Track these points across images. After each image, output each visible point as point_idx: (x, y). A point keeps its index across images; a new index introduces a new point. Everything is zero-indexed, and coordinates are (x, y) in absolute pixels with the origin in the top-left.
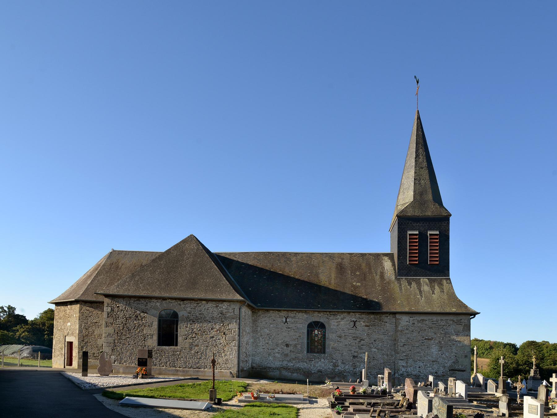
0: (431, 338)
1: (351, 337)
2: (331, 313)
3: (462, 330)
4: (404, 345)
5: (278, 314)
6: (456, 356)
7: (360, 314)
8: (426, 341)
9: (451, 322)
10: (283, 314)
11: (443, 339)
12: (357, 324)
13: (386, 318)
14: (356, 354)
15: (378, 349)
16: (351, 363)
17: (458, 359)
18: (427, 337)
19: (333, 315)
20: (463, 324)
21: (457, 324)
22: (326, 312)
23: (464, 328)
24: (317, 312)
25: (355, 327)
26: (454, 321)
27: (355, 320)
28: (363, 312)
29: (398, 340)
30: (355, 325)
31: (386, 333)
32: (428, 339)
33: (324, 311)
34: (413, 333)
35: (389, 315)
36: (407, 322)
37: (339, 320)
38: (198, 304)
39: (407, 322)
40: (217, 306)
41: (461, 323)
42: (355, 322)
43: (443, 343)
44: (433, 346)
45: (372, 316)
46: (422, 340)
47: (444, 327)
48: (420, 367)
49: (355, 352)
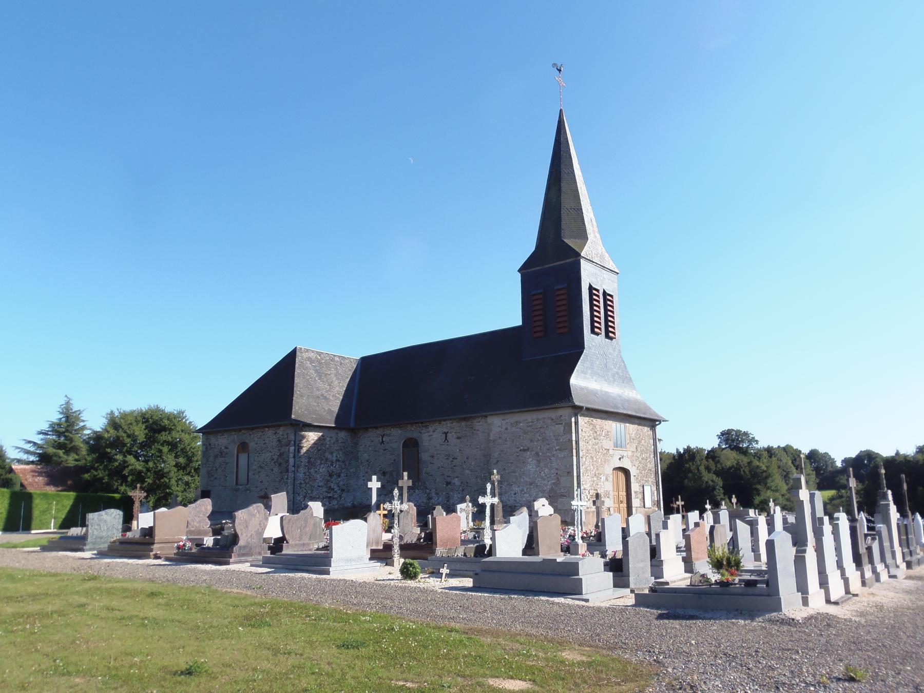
0: (526, 448)
1: (443, 456)
2: (423, 425)
3: (562, 432)
4: (498, 461)
5: (375, 432)
6: (557, 474)
7: (451, 421)
8: (521, 452)
9: (550, 421)
10: (380, 431)
11: (540, 449)
12: (449, 436)
13: (477, 424)
14: (448, 480)
15: (471, 471)
16: (444, 493)
17: (559, 478)
18: (522, 448)
19: (425, 426)
20: (564, 423)
21: (557, 424)
22: (418, 423)
23: (564, 429)
24: (409, 425)
25: (446, 441)
26: (553, 420)
27: (446, 431)
28: (455, 419)
29: (490, 455)
30: (446, 439)
31: (478, 447)
32: (524, 450)
33: (416, 423)
34: (506, 443)
35: (482, 419)
36: (499, 426)
37: (430, 434)
38: (263, 432)
39: (499, 426)
40: (275, 433)
41: (561, 420)
42: (446, 434)
43: (540, 454)
44: (529, 460)
45: (463, 424)
46: (517, 453)
47: (542, 430)
48: (515, 494)
49: (448, 476)
